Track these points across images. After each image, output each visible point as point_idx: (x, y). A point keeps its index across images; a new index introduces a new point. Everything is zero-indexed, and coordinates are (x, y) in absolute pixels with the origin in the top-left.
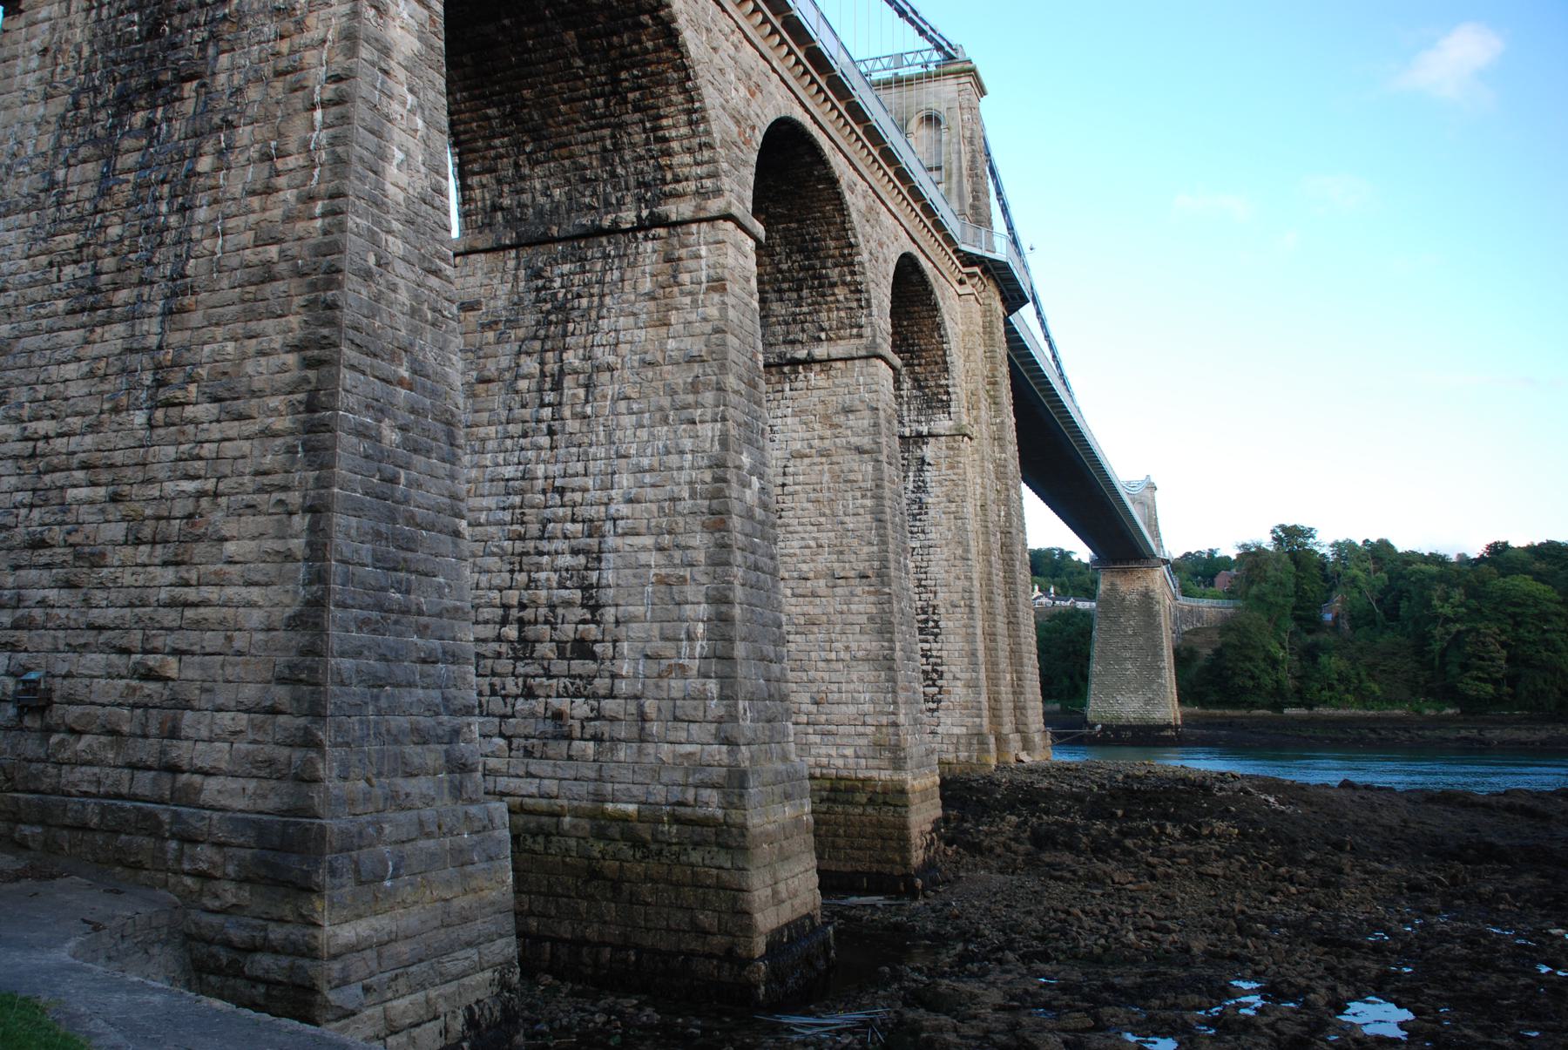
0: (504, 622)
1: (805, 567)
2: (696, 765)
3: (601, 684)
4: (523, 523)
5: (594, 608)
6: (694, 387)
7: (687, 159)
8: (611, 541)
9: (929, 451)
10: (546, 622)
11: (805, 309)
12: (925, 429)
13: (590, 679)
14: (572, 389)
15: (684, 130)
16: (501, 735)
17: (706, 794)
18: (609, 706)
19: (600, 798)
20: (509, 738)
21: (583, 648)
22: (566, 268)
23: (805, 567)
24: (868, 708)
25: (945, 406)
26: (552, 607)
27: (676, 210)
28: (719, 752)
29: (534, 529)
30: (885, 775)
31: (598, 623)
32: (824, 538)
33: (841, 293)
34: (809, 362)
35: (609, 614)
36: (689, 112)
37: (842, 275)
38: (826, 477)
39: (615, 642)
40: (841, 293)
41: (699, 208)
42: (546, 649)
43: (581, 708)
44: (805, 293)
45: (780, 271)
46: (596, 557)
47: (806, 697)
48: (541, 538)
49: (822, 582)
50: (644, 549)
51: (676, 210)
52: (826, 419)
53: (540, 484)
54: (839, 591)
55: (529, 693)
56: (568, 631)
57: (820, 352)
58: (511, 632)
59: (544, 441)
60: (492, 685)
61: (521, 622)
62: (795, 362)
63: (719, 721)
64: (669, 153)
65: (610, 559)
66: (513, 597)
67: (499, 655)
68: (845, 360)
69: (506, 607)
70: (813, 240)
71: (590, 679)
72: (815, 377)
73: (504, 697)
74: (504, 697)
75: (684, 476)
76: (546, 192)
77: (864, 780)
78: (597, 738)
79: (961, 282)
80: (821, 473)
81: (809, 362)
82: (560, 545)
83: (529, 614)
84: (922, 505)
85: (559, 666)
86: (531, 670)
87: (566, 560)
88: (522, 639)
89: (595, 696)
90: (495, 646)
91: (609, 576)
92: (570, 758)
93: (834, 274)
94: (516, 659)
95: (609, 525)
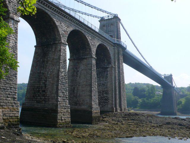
0: (37, 88)
2: (53, 104)
3: (46, 95)
5: (45, 86)
6: (57, 62)
7: (58, 36)
8: (48, 79)
9: (108, 69)
12: (108, 67)
13: (45, 94)
14: (45, 63)
15: (57, 33)
16: (36, 101)
17: (54, 107)
18: (46, 97)
20: (37, 101)
21: (44, 91)
22: (46, 49)
24: (88, 101)
25: (110, 63)
26: (42, 87)
27: (57, 42)
28: (55, 102)
29: (41, 78)
30: (90, 110)
31: (46, 88)
33: (88, 49)
34: (84, 58)
35: (47, 88)
36: (57, 31)
39: (47, 90)
40: (88, 49)
41: (58, 42)
42: (41, 91)
43: (44, 98)
46: (46, 81)
49: (84, 86)
50: (51, 80)
51: (57, 42)
53: (42, 73)
55: (39, 96)
56: (43, 89)
58: (38, 89)
59: (42, 68)
63: (56, 99)
64: (56, 36)
65: (47, 81)
66: (38, 85)
67: (37, 92)
69: (37, 86)
71: (45, 94)
75: (55, 72)
77: (88, 110)
78: (45, 101)
79: (114, 47)
84: (107, 77)
85: (42, 93)
86: (39, 94)
87: (43, 81)
88: (39, 90)
90: (36, 91)
91: (47, 83)
95: (48, 78)
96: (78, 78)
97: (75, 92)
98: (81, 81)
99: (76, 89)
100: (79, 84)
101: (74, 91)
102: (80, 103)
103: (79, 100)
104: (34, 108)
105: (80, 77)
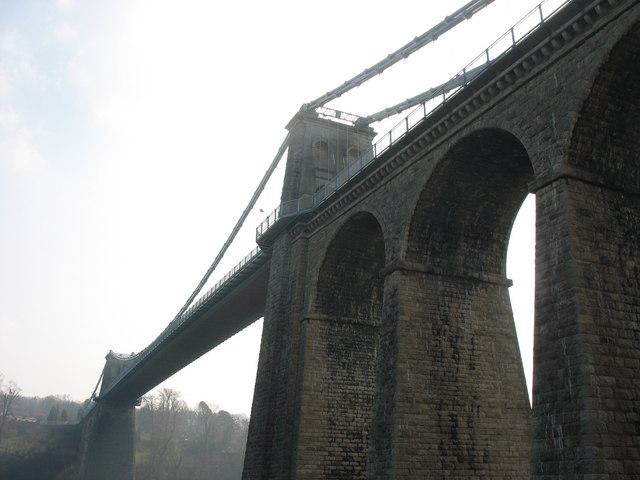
1: (491, 400)
23: (491, 400)
32: (498, 383)
34: (478, 281)
38: (493, 349)
40: (495, 246)
62: (472, 279)
76: (614, 161)
93: (495, 236)
96: (464, 367)
97: (464, 437)
98: (483, 387)
99: (462, 422)
100: (475, 397)
101: (454, 435)
105: (472, 366)
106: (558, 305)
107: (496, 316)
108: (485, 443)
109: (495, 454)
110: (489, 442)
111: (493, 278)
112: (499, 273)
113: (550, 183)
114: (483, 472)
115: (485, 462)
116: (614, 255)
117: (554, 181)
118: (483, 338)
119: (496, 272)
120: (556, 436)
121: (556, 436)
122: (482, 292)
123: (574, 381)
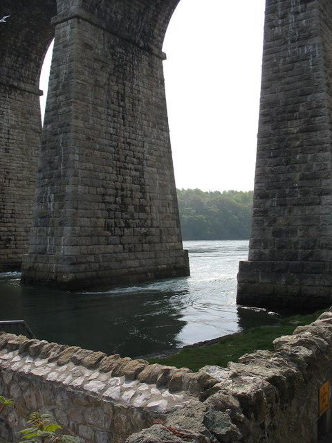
1: (19, 175)
4: (118, 154)
10: (130, 197)
11: (17, 66)
16: (121, 244)
19: (157, 264)
23: (19, 175)
32: (26, 164)
34: (16, 88)
37: (36, 58)
38: (24, 139)
42: (131, 208)
44: (20, 59)
45: (16, 46)
47: (22, 229)
48: (125, 162)
52: (23, 115)
54: (32, 187)
55: (128, 226)
57: (22, 86)
60: (115, 223)
61: (123, 196)
68: (29, 92)
70: (35, 40)
71: (145, 220)
72: (17, 95)
73: (120, 228)
74: (120, 228)
76: (116, 13)
80: (22, 137)
81: (16, 88)
82: (130, 166)
83: (125, 193)
86: (128, 216)
88: (123, 203)
89: (147, 227)
92: (143, 251)
93: (34, 56)
94: (122, 211)
98: (14, 166)
100: (8, 173)
102: (19, 238)
103: (14, 229)
104: (126, 271)
106: (61, 111)
107: (28, 116)
108: (13, 204)
109: (20, 212)
110: (16, 204)
111: (29, 87)
112: (34, 84)
113: (66, 20)
114: (10, 224)
115: (12, 217)
116: (105, 80)
117: (70, 19)
118: (17, 131)
119: (31, 83)
120: (50, 202)
121: (50, 202)
122: (19, 98)
123: (64, 165)
